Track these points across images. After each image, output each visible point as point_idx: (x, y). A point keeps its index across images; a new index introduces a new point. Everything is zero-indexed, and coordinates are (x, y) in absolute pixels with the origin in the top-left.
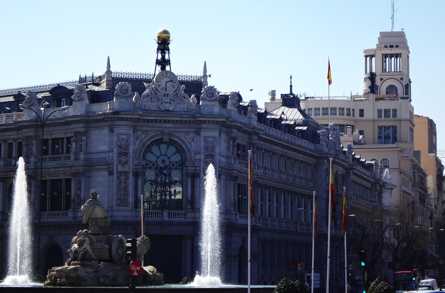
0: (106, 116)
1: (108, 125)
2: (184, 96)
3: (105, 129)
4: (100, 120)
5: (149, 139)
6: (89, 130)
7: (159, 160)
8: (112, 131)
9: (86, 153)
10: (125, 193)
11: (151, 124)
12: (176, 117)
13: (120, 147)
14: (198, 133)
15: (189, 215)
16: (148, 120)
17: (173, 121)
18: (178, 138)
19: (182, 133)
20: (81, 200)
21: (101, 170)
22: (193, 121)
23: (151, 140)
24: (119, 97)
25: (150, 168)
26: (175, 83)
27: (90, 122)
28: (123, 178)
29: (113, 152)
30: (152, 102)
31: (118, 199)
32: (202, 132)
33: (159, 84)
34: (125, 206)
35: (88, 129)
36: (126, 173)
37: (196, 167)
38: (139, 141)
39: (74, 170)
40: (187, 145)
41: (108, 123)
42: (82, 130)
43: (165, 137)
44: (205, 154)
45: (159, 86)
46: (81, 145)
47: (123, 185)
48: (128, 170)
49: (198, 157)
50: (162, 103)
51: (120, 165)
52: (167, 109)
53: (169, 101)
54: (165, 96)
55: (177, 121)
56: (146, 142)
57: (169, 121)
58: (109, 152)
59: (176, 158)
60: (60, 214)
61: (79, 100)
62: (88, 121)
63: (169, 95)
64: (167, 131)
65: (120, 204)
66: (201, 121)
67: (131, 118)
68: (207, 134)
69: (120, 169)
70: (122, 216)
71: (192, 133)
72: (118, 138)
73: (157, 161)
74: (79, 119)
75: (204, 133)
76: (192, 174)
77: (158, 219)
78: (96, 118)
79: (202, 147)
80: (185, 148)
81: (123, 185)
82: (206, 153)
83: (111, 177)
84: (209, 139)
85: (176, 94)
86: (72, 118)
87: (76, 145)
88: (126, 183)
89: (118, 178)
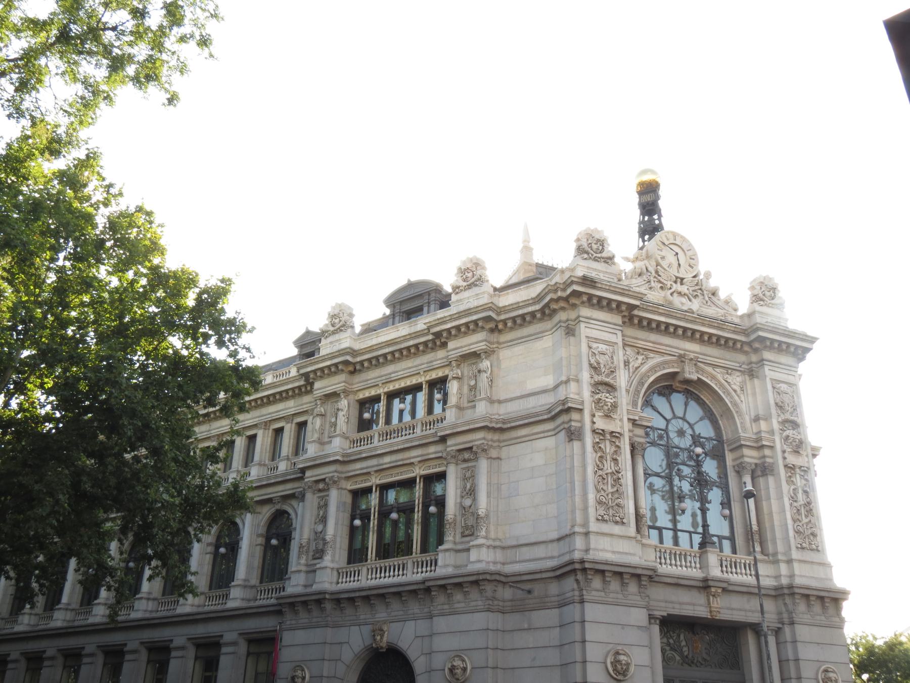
0: (560, 294)
1: (560, 322)
4: (533, 314)
5: (653, 369)
7: (670, 427)
8: (570, 332)
9: (491, 401)
10: (615, 489)
11: (653, 337)
12: (710, 326)
13: (595, 368)
14: (752, 373)
15: (763, 569)
16: (650, 321)
17: (703, 334)
18: (713, 378)
19: (718, 370)
20: (478, 517)
21: (537, 436)
22: (743, 343)
23: (656, 371)
24: (586, 256)
25: (653, 444)
27: (500, 326)
28: (609, 448)
29: (577, 381)
30: (651, 288)
31: (600, 503)
32: (766, 368)
33: (663, 253)
34: (616, 523)
36: (615, 436)
37: (763, 446)
38: (631, 370)
39: (455, 445)
40: (732, 397)
41: (556, 318)
42: (482, 346)
43: (687, 369)
44: (780, 420)
45: (663, 258)
46: (473, 389)
47: (609, 467)
48: (618, 430)
49: (763, 425)
50: (672, 294)
51: (601, 414)
52: (685, 308)
53: (687, 292)
54: (675, 282)
55: (711, 335)
56: (646, 375)
57: (694, 331)
58: (567, 382)
59: (705, 430)
60: (410, 565)
61: (470, 287)
62: (497, 326)
63: (685, 281)
64: (692, 355)
65: (606, 517)
66: (762, 339)
67: (619, 303)
68: (777, 374)
69: (601, 424)
70: (613, 552)
71: (738, 374)
72: (590, 348)
73: (666, 430)
74: (474, 317)
75: (772, 373)
76: (753, 466)
77: (696, 573)
78: (521, 312)
79: (772, 402)
80: (729, 405)
81: (609, 467)
82: (783, 417)
83: (576, 444)
84: (784, 387)
85: (697, 285)
86: (456, 319)
87: (460, 389)
88: (615, 460)
89: (597, 447)
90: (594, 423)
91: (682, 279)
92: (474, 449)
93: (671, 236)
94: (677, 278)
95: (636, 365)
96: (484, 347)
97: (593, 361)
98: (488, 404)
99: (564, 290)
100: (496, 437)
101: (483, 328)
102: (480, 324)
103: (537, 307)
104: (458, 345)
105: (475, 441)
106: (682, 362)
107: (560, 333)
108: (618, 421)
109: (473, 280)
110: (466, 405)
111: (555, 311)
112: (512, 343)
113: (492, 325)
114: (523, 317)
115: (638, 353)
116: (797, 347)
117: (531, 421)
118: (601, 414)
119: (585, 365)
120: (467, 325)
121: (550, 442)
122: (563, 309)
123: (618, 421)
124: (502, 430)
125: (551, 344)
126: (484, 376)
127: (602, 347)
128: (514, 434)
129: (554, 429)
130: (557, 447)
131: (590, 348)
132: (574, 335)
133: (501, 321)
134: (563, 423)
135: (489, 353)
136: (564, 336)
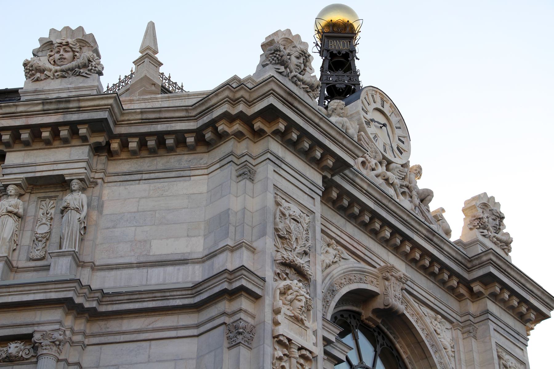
0: (241, 107)
1: (231, 154)
2: (423, 196)
3: (192, 178)
6: (102, 179)
8: (247, 173)
18: (419, 319)
26: (403, 142)
27: (115, 145)
35: (97, 176)
54: (381, 163)
62: (108, 144)
63: (392, 166)
69: (286, 329)
72: (278, 204)
78: (160, 127)
90: (276, 323)
91: (389, 162)
92: (37, 337)
93: (378, 98)
94: (384, 158)
95: (328, 261)
96: (83, 171)
97: (281, 226)
98: (74, 265)
99: (250, 103)
100: (80, 325)
101: (84, 139)
102: (83, 131)
103: (192, 125)
104: (27, 161)
105: (39, 324)
106: (387, 279)
107: (231, 170)
108: (310, 332)
109: (74, 63)
110: (23, 263)
111: (222, 137)
112: (129, 177)
113: (101, 139)
114: (161, 137)
115: (329, 245)
116: (531, 307)
117: (156, 306)
118: (289, 313)
119: (270, 230)
120: (55, 127)
121: (188, 348)
122: (239, 136)
123: (310, 332)
124: (93, 315)
125: (204, 189)
126: (73, 217)
127: (295, 210)
128: (114, 325)
129: (198, 326)
130: (199, 357)
131: (278, 204)
132: (252, 180)
133: (120, 136)
134: (224, 314)
135: (86, 184)
136: (234, 177)
